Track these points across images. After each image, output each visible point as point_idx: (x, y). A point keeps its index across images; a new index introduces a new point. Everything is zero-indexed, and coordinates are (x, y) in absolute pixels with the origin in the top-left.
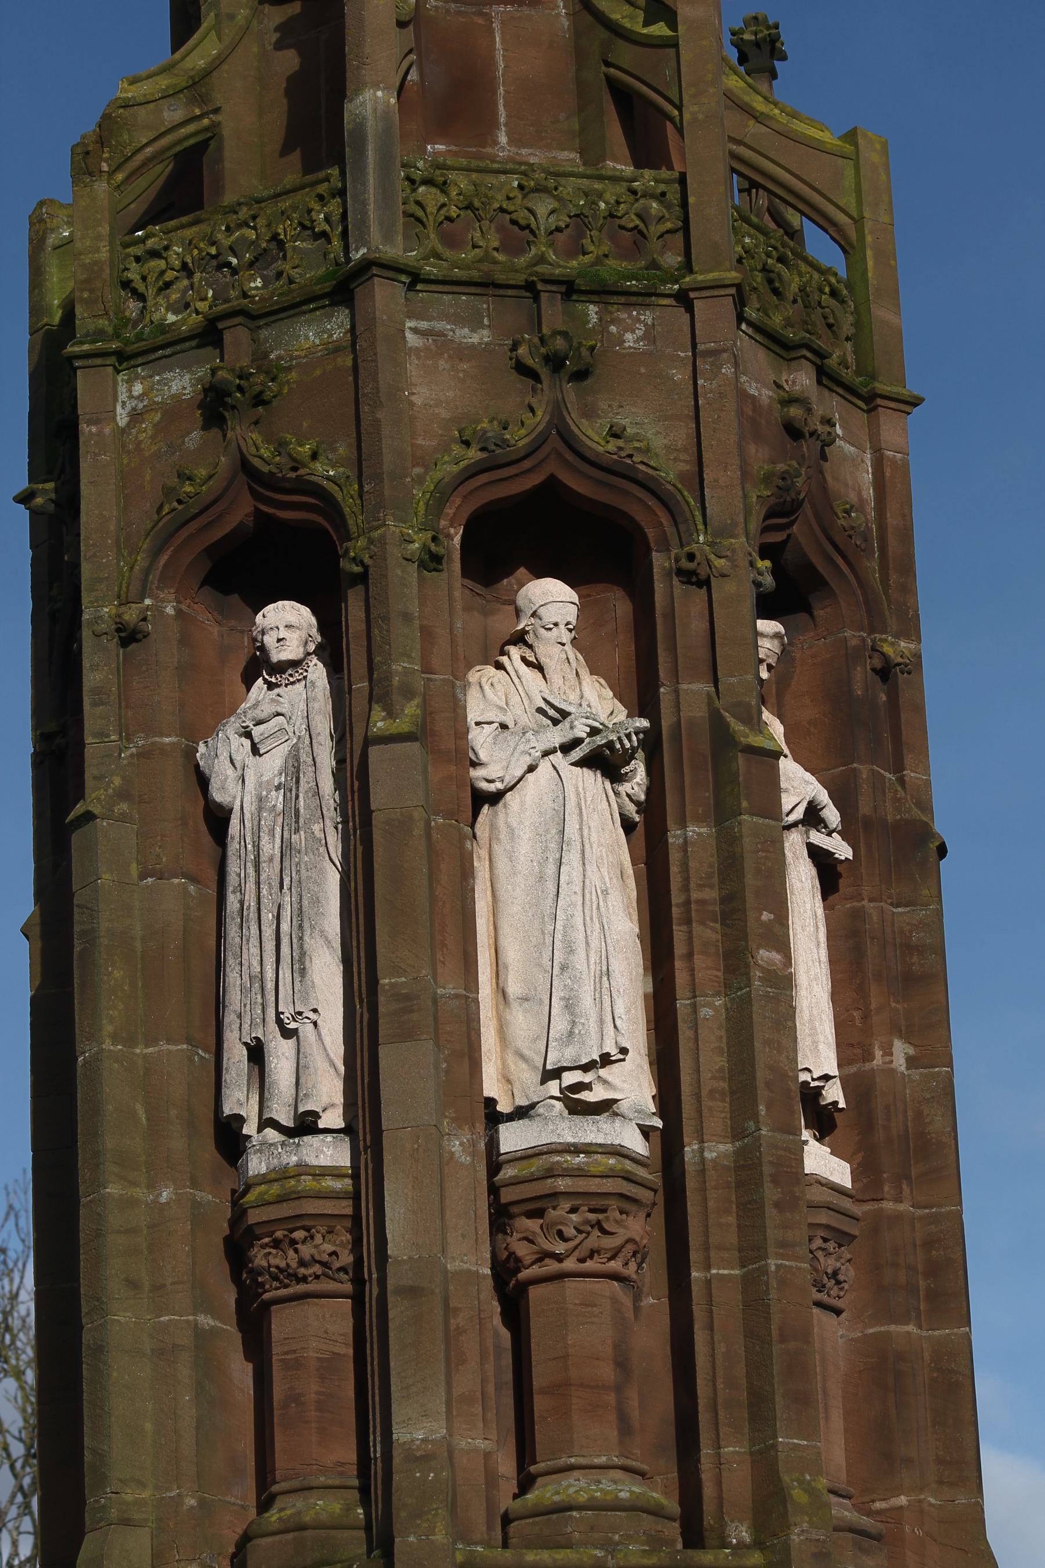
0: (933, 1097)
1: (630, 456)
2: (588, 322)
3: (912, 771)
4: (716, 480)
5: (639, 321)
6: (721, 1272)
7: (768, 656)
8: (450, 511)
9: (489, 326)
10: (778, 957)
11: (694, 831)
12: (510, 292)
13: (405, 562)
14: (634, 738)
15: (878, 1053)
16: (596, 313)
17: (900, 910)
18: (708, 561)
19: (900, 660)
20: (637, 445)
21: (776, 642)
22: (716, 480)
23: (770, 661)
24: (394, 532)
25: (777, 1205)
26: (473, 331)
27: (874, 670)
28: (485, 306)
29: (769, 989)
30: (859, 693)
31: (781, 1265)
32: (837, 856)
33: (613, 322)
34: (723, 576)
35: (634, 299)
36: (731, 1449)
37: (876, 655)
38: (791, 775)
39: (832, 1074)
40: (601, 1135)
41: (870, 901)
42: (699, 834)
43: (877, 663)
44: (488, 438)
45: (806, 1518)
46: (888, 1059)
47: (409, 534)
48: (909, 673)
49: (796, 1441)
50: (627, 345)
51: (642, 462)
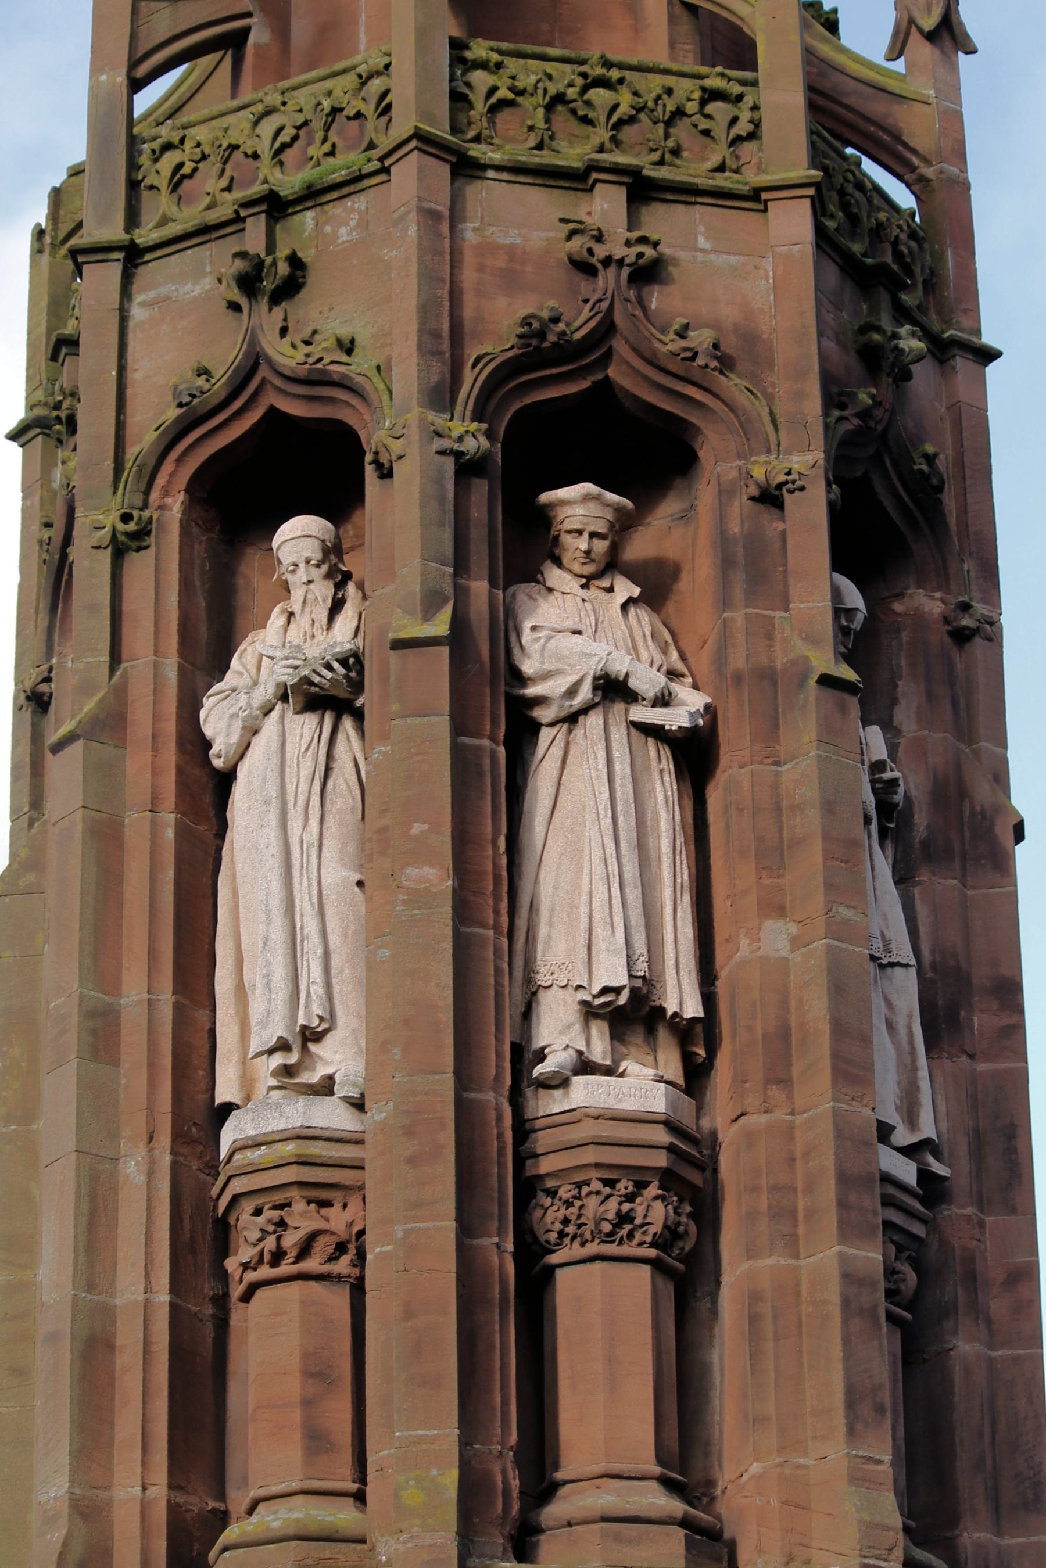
0: (811, 978)
1: (321, 359)
2: (304, 231)
3: (802, 602)
4: (400, 355)
5: (353, 210)
6: (385, 1249)
7: (588, 524)
8: (161, 480)
9: (211, 273)
10: (432, 871)
11: (379, 753)
12: (229, 230)
13: (95, 551)
14: (336, 665)
15: (744, 943)
16: (313, 219)
17: (787, 767)
18: (385, 446)
19: (782, 478)
20: (324, 345)
21: (592, 505)
22: (400, 355)
23: (592, 528)
24: (83, 523)
25: (411, 1161)
26: (195, 283)
27: (752, 499)
28: (208, 253)
29: (416, 912)
30: (736, 530)
31: (412, 1229)
32: (667, 727)
33: (325, 223)
34: (401, 457)
35: (345, 190)
36: (386, 1452)
37: (750, 482)
38: (565, 653)
39: (617, 985)
40: (283, 1120)
41: (741, 767)
42: (385, 754)
43: (754, 491)
44: (181, 392)
45: (418, 1522)
46: (755, 946)
47: (99, 521)
48: (802, 489)
49: (420, 1432)
50: (340, 241)
51: (333, 362)
